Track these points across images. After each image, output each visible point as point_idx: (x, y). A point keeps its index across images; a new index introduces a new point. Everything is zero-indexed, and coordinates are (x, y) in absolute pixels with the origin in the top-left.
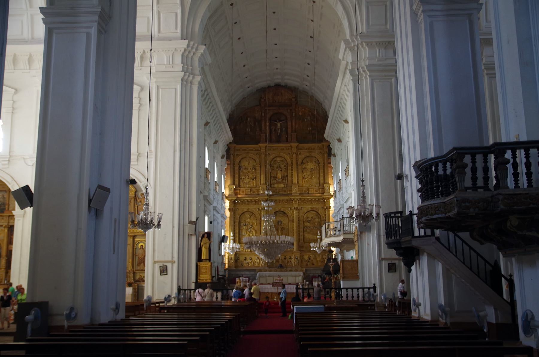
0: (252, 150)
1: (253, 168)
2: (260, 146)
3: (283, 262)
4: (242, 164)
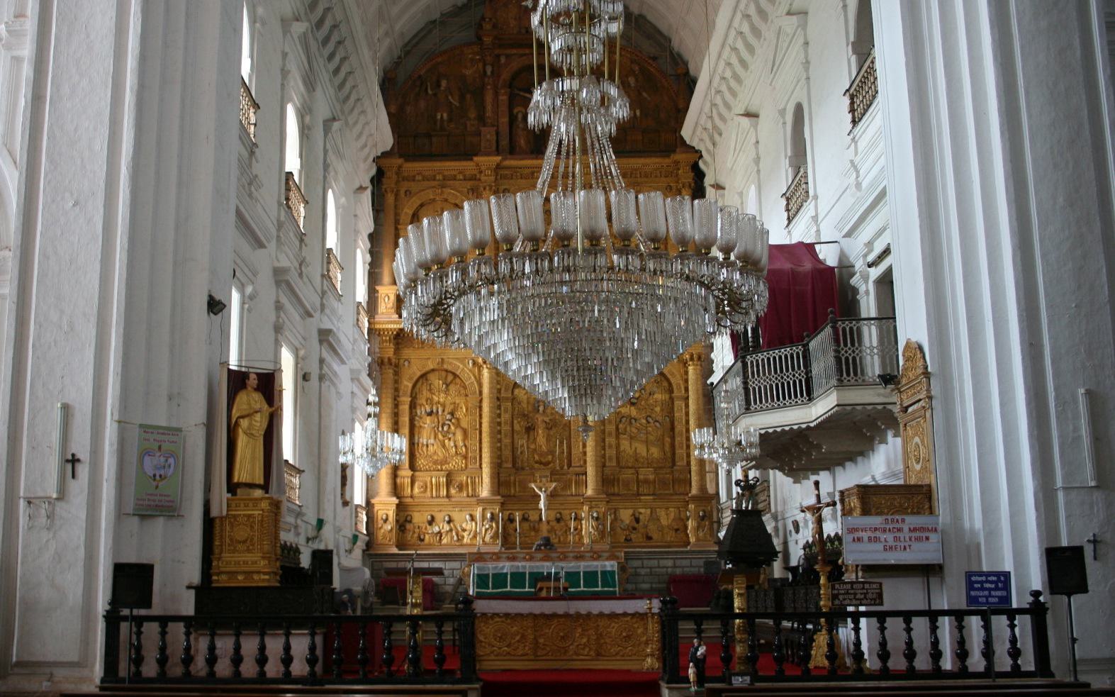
0: (454, 178)
2: (477, 165)
3: (552, 530)
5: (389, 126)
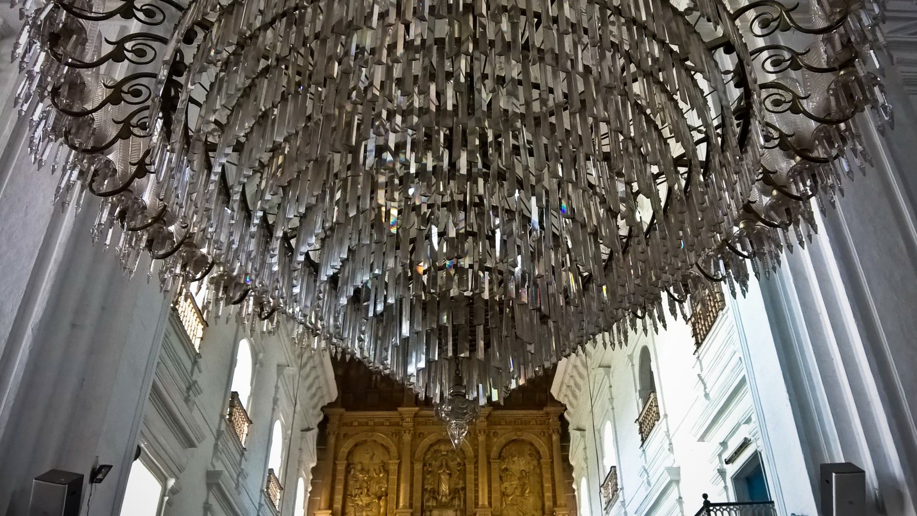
1: (381, 468)
2: (401, 414)
4: (356, 459)
5: (334, 381)
